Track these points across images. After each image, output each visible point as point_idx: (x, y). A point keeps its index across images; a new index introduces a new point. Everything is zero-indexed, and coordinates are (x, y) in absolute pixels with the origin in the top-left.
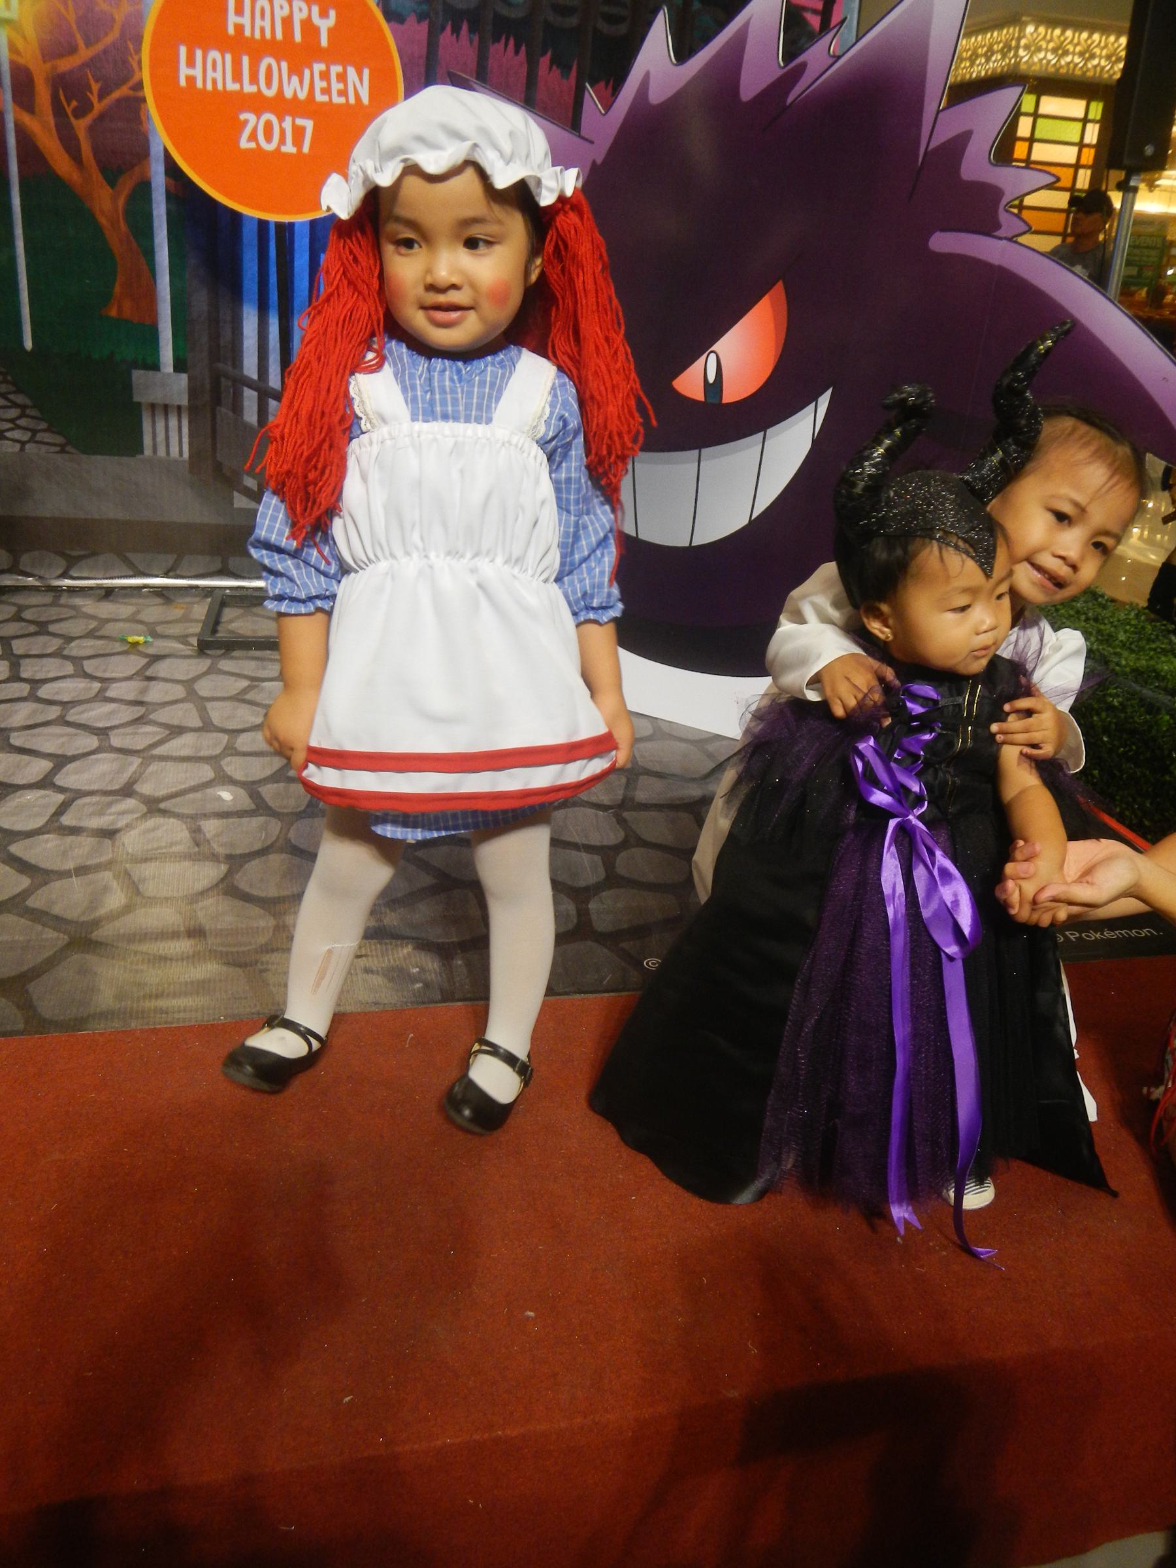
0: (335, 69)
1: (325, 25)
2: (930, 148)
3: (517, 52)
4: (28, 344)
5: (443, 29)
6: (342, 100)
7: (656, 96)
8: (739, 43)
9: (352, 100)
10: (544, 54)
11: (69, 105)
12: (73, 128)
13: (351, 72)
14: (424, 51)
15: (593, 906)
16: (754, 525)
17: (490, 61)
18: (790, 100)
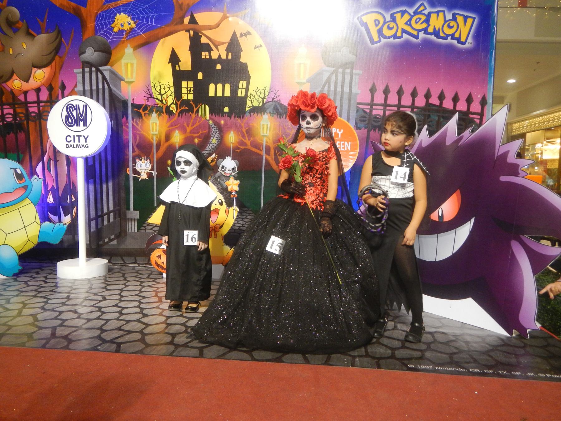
0: (342, 142)
1: (340, 133)
5: (371, 130)
6: (343, 149)
7: (424, 145)
8: (445, 133)
9: (346, 149)
11: (278, 153)
12: (278, 158)
13: (346, 143)
14: (366, 135)
15: (396, 352)
16: (454, 255)
18: (459, 145)
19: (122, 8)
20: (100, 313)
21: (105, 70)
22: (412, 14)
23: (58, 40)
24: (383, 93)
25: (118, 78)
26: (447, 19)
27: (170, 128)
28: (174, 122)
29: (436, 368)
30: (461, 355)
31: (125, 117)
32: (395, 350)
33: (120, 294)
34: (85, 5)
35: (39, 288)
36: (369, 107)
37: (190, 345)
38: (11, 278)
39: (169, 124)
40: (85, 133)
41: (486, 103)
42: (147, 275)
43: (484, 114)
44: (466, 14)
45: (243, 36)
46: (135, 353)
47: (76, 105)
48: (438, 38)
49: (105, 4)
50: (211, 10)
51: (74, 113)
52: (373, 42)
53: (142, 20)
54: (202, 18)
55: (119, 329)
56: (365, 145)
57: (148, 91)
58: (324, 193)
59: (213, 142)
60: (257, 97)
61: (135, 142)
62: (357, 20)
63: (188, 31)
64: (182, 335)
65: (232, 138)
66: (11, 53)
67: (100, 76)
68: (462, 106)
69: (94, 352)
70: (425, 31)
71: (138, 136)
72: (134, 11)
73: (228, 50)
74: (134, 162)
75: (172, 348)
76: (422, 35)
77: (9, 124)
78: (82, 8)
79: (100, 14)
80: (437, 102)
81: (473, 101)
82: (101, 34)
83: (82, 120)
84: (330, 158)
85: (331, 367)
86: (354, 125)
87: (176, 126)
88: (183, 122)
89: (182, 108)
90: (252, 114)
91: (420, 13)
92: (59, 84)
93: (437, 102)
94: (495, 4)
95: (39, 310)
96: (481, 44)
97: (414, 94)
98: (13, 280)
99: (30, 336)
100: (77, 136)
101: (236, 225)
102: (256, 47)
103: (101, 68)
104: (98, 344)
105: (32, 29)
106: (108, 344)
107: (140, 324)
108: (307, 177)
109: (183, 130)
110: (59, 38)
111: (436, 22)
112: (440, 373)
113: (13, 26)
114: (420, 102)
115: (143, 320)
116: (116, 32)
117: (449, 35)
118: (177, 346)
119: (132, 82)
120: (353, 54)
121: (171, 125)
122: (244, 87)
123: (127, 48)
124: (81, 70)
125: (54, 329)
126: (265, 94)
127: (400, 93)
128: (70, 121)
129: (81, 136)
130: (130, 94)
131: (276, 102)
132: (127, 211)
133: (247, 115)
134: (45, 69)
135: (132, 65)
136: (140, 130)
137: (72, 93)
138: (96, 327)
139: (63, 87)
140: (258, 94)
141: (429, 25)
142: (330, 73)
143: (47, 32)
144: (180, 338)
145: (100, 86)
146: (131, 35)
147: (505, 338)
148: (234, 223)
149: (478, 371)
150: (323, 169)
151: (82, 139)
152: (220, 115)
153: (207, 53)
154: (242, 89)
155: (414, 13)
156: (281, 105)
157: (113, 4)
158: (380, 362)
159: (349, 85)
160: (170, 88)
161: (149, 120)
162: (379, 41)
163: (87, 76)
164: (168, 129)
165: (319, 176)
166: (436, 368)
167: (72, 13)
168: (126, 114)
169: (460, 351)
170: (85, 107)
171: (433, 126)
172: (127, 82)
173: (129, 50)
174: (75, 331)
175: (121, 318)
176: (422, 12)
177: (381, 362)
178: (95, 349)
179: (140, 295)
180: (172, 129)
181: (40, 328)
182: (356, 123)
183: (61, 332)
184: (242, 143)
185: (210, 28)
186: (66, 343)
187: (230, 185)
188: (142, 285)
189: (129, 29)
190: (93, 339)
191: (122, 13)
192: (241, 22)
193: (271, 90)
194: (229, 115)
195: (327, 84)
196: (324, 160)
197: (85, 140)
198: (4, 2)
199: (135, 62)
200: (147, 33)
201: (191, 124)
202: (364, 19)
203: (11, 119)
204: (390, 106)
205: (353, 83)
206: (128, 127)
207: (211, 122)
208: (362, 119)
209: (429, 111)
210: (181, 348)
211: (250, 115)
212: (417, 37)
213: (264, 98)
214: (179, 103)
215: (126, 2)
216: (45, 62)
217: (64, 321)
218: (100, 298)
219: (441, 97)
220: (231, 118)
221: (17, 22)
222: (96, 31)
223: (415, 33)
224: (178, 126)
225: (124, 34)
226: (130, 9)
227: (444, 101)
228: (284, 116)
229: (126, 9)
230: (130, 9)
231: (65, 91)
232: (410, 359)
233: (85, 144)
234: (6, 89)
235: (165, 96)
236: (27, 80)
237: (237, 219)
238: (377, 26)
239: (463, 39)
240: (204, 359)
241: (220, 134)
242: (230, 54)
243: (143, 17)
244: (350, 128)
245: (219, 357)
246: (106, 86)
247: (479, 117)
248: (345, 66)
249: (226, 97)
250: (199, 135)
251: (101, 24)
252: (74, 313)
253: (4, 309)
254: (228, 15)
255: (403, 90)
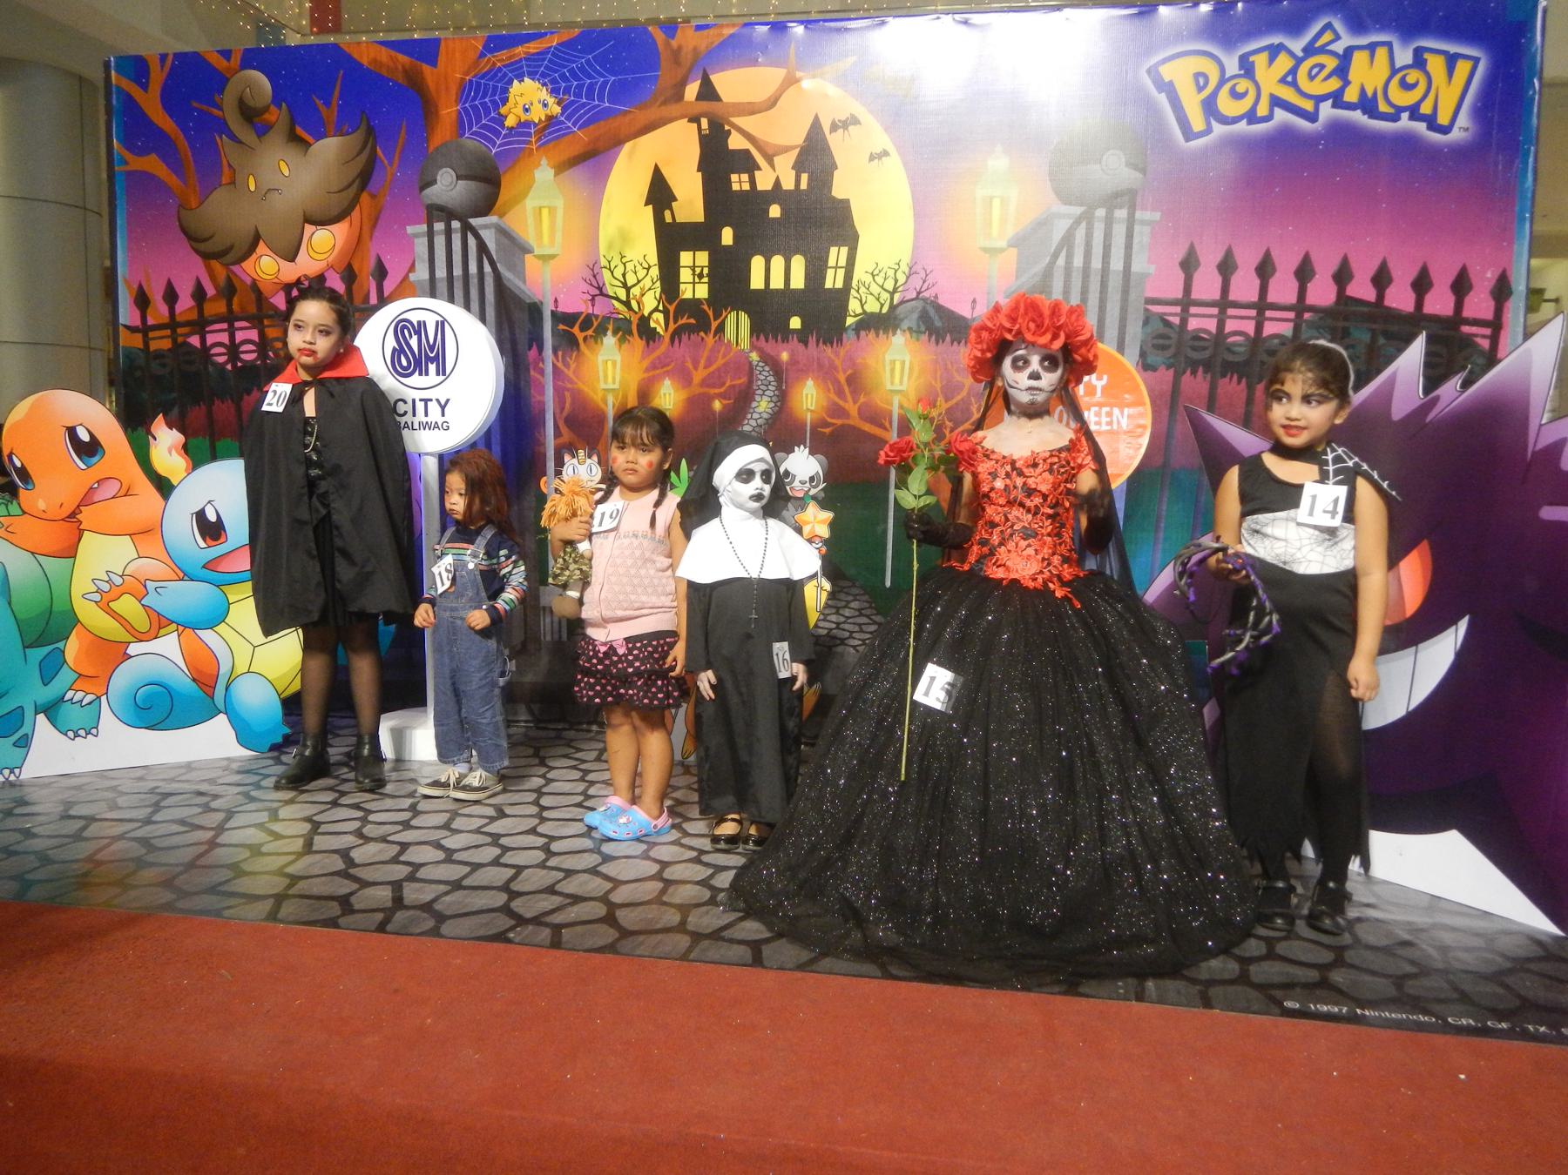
0: (1105, 410)
2: (1537, 448)
3: (1239, 382)
4: (888, 584)
5: (1184, 372)
6: (1109, 428)
9: (1115, 427)
10: (1260, 381)
13: (1116, 411)
15: (1253, 968)
17: (1219, 390)
19: (527, 65)
20: (497, 851)
21: (486, 227)
22: (1300, 54)
23: (367, 151)
24: (1216, 272)
25: (516, 247)
26: (1398, 64)
27: (651, 374)
28: (659, 358)
29: (1359, 1011)
30: (1426, 982)
31: (535, 346)
32: (1249, 965)
33: (536, 803)
34: (432, 60)
35: (338, 782)
36: (1178, 309)
37: (726, 934)
38: (265, 755)
39: (646, 363)
40: (440, 393)
41: (1510, 293)
42: (595, 754)
43: (1504, 325)
44: (1453, 48)
45: (840, 127)
46: (600, 950)
47: (419, 323)
48: (1371, 117)
49: (482, 55)
50: (754, 63)
51: (414, 342)
52: (1189, 134)
53: (578, 95)
54: (732, 84)
55: (551, 890)
56: (1166, 413)
57: (592, 279)
58: (1062, 555)
59: (761, 409)
60: (875, 289)
61: (563, 409)
62: (1146, 75)
63: (695, 119)
64: (704, 909)
65: (809, 398)
66: (252, 188)
67: (472, 241)
68: (1439, 303)
69: (502, 946)
70: (1337, 99)
71: (567, 394)
72: (556, 71)
73: (799, 167)
74: (560, 463)
75: (683, 941)
76: (1326, 110)
77: (249, 368)
78: (426, 68)
79: (470, 81)
80: (1369, 294)
81: (1471, 287)
82: (475, 133)
83: (432, 360)
84: (1081, 467)
85: (1083, 1000)
86: (1136, 357)
87: (665, 369)
88: (684, 356)
89: (680, 322)
90: (863, 333)
91: (1323, 50)
92: (372, 263)
93: (1369, 294)
94: (1536, 17)
95: (351, 840)
96: (1495, 131)
97: (1304, 273)
98: (271, 762)
99: (345, 902)
100: (421, 400)
101: (821, 624)
102: (872, 158)
103: (471, 220)
104: (507, 926)
105: (304, 129)
106: (530, 927)
107: (598, 881)
108: (1019, 515)
109: (684, 378)
110: (369, 145)
111: (1367, 74)
112: (1370, 1025)
113: (256, 120)
114: (1322, 293)
115: (604, 869)
116: (512, 128)
117: (1403, 109)
118: (697, 937)
119: (552, 257)
120: (1136, 167)
121: (653, 367)
122: (842, 262)
123: (540, 168)
124: (424, 227)
125: (397, 886)
126: (896, 281)
127: (1265, 270)
128: (404, 363)
129: (431, 400)
130: (548, 286)
131: (925, 300)
132: (542, 588)
133: (849, 337)
134: (335, 227)
135: (552, 210)
136: (574, 378)
137: (405, 289)
138: (494, 885)
139: (381, 272)
140: (880, 280)
141: (1347, 83)
142: (1071, 221)
143: (339, 132)
144: (701, 917)
145: (473, 268)
146: (550, 134)
147: (1549, 940)
148: (818, 620)
149: (1469, 1025)
150: (1060, 494)
151: (433, 406)
152: (779, 338)
153: (745, 177)
154: (836, 268)
155: (1305, 50)
156: (940, 309)
157: (503, 54)
158: (1210, 994)
159: (1123, 251)
160: (648, 269)
161: (597, 355)
162: (1209, 130)
163: (440, 241)
164: (646, 375)
165: (1050, 511)
166: (1359, 1011)
167: (401, 79)
168: (536, 340)
169: (1424, 971)
170: (441, 325)
171: (1358, 357)
172: (541, 257)
173: (544, 174)
174: (447, 893)
175: (552, 862)
176: (1331, 47)
177: (1214, 992)
178: (501, 937)
179: (585, 804)
180: (654, 376)
181: (365, 884)
182: (1143, 355)
183: (412, 894)
184: (837, 411)
185: (751, 109)
186: (430, 923)
187: (807, 523)
188: (586, 778)
189: (543, 119)
190: (494, 915)
191: (526, 79)
192: (832, 90)
193: (913, 270)
194: (803, 336)
195: (1065, 250)
196: (1062, 470)
197: (439, 409)
198: (233, 59)
199: (559, 203)
200: (592, 127)
201: (703, 362)
202: (1167, 72)
203: (255, 355)
204: (1236, 305)
205: (1135, 247)
206: (542, 372)
207: (754, 356)
208: (1161, 341)
209: (1346, 319)
210: (706, 943)
211: (858, 337)
212: (1312, 117)
213: (895, 290)
214: (672, 308)
215: (537, 48)
216: (335, 212)
217: (417, 866)
218: (491, 812)
219: (1381, 279)
220: (806, 344)
221: (266, 109)
222: (461, 128)
223: (1308, 106)
224: (669, 368)
225: (532, 131)
226: (547, 67)
227: (1387, 291)
228: (948, 338)
229: (535, 66)
230: (547, 67)
231: (385, 283)
232: (1289, 986)
233: (440, 420)
234: (242, 281)
235: (636, 291)
236: (291, 256)
237: (824, 608)
238: (1200, 89)
239: (1443, 120)
240: (764, 971)
241: (779, 388)
242: (804, 177)
243: (580, 87)
244: (1129, 372)
245: (801, 967)
246: (487, 268)
247: (1488, 331)
248: (1113, 200)
249: (795, 291)
250: (725, 392)
251: (474, 107)
252: (436, 848)
253: (269, 835)
254: (799, 74)
255: (1273, 264)
